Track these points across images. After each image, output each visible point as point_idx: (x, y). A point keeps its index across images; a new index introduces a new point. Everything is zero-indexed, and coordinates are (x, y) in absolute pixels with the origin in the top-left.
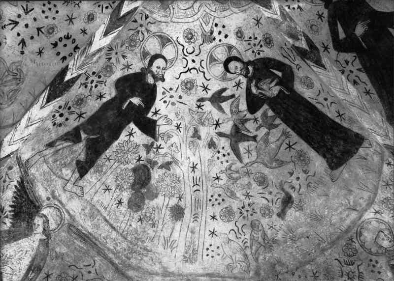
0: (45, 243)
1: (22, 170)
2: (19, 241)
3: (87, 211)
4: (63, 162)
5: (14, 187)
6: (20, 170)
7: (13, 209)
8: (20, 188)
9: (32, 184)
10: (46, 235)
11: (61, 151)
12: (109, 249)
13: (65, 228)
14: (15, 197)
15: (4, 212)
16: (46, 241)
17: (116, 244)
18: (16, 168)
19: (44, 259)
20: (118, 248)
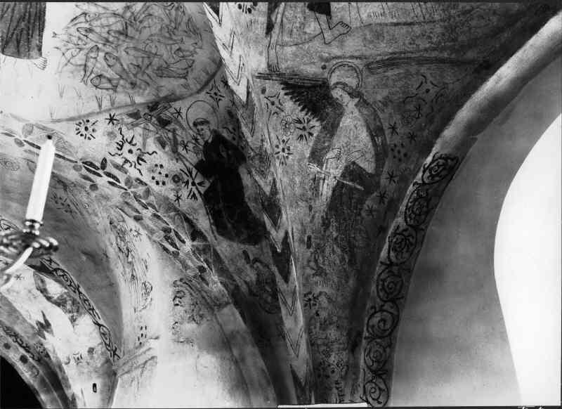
0: (363, 103)
1: (274, 78)
2: (341, 125)
3: (368, 37)
4: (298, 25)
5: (285, 97)
6: (273, 80)
7: (306, 110)
9: (296, 75)
10: (356, 97)
11: (284, 19)
12: (426, 50)
13: (365, 73)
14: (296, 101)
15: (303, 121)
16: (362, 100)
17: (430, 38)
18: (268, 84)
19: (376, 117)
20: (435, 40)
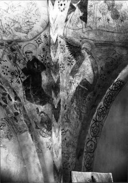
0: (92, 57)
2: (83, 63)
3: (98, 34)
4: (75, 23)
5: (66, 47)
7: (72, 55)
8: (69, 46)
9: (71, 41)
11: (72, 19)
12: (117, 42)
13: (94, 46)
14: (69, 50)
19: (96, 63)
20: (121, 39)
